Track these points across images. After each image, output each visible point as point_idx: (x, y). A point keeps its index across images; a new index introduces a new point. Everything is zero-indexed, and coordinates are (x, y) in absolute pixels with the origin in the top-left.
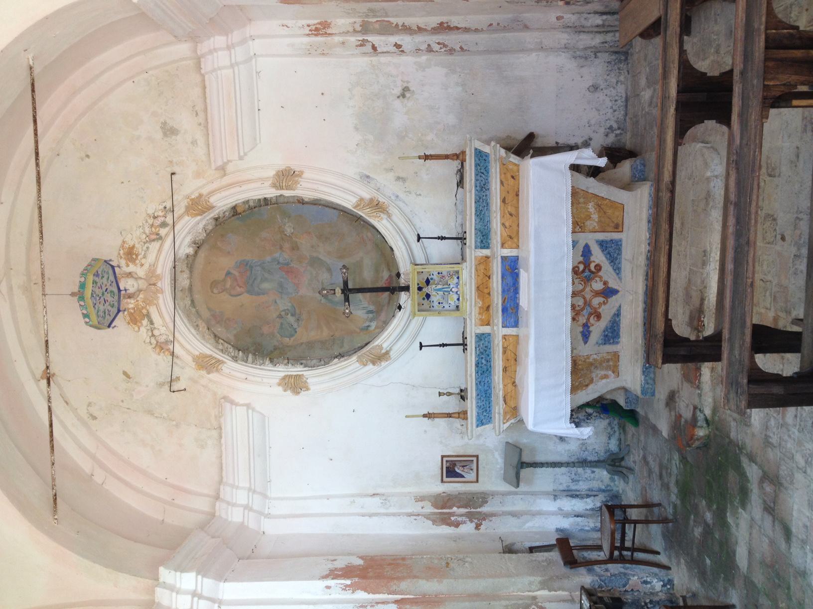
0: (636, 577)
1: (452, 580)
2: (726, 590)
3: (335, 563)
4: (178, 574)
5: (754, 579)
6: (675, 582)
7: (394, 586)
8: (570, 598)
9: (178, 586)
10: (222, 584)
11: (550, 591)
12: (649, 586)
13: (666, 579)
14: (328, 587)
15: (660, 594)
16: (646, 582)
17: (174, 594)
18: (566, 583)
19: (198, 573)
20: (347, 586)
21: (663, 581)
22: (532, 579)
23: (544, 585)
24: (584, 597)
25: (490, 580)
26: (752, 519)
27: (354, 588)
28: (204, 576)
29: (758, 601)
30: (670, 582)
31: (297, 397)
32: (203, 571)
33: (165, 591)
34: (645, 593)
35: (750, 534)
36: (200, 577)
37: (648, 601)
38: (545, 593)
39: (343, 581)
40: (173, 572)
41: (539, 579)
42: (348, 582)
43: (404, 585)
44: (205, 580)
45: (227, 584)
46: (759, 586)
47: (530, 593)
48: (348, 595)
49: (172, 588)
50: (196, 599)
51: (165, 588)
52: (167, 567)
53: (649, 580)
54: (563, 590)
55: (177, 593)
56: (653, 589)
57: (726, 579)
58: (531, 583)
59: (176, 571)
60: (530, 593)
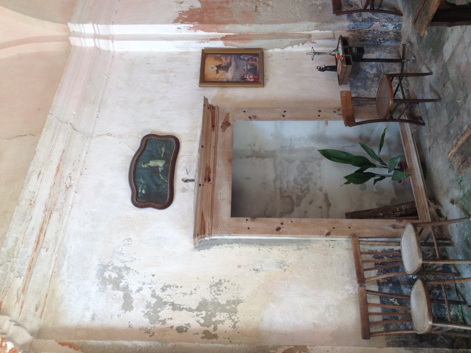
0: (378, 23)
1: (258, 25)
2: (430, 60)
3: (182, 5)
4: (81, 25)
5: (449, 70)
6: (403, 26)
7: (221, 27)
8: (332, 36)
9: (83, 32)
10: (111, 26)
11: (320, 30)
12: (385, 28)
13: (397, 24)
14: (179, 28)
15: (391, 33)
16: (383, 26)
17: (82, 39)
18: (332, 26)
19: (93, 23)
20: (191, 28)
21: (395, 25)
22: (310, 23)
23: (316, 28)
24: (340, 46)
25: (283, 25)
26: (462, 37)
27: (196, 29)
28: (98, 24)
29: (446, 83)
30: (400, 26)
31: (130, 204)
32: (95, 21)
33: (75, 38)
34: (381, 32)
35: (458, 44)
36: (95, 25)
37: (381, 39)
38: (317, 31)
39: (188, 25)
40: (77, 25)
41: (315, 24)
42: (192, 26)
43: (227, 27)
44: (99, 26)
45: (114, 26)
46: (451, 77)
47: (308, 32)
48: (192, 33)
49: (80, 35)
50: (96, 40)
51: (75, 36)
52: (71, 23)
53: (386, 24)
54: (329, 29)
55: (84, 38)
56: (388, 29)
57: (433, 52)
58: (309, 26)
59: (79, 23)
60: (308, 32)
